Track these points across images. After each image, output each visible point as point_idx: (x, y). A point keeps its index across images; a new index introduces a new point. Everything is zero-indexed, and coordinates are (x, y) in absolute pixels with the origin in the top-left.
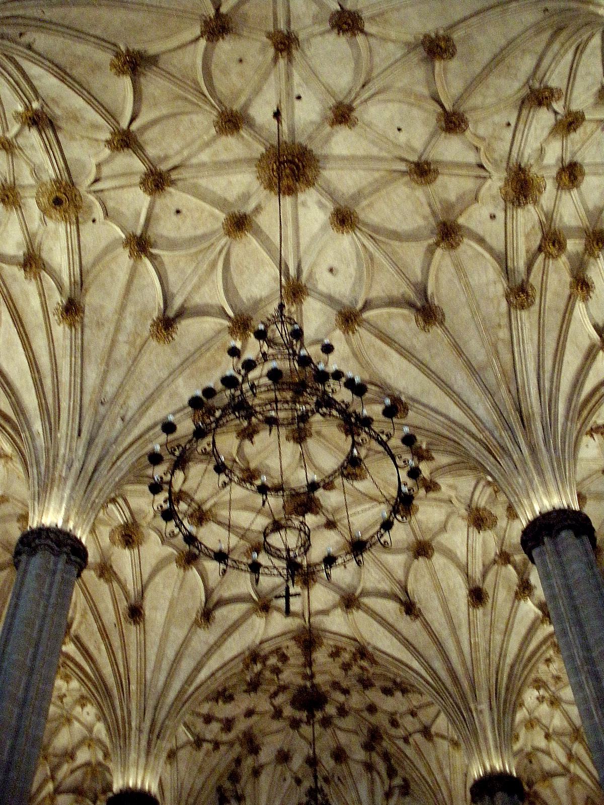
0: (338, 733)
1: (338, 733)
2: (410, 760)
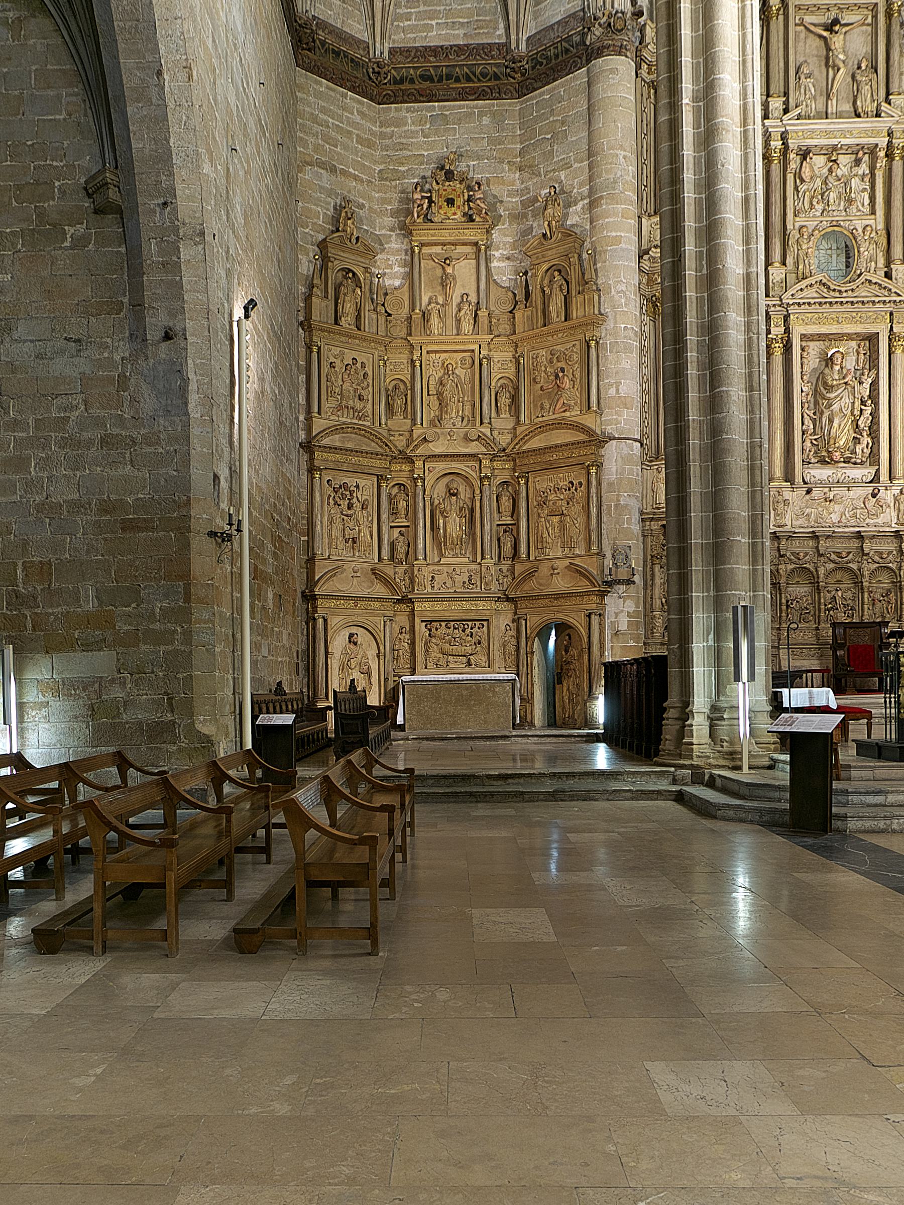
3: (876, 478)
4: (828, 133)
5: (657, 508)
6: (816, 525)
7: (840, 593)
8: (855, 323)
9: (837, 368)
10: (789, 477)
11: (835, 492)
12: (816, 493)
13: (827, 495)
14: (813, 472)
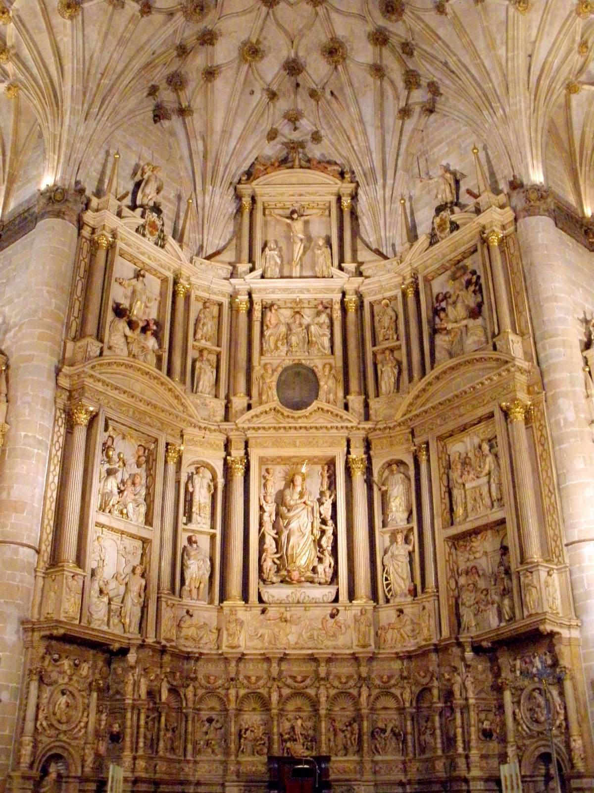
0: (334, 16)
1: (334, 16)
2: (444, 42)
3: (336, 600)
4: (285, 290)
6: (271, 646)
7: (299, 722)
8: (313, 446)
9: (298, 489)
10: (245, 597)
11: (293, 612)
12: (272, 612)
13: (284, 615)
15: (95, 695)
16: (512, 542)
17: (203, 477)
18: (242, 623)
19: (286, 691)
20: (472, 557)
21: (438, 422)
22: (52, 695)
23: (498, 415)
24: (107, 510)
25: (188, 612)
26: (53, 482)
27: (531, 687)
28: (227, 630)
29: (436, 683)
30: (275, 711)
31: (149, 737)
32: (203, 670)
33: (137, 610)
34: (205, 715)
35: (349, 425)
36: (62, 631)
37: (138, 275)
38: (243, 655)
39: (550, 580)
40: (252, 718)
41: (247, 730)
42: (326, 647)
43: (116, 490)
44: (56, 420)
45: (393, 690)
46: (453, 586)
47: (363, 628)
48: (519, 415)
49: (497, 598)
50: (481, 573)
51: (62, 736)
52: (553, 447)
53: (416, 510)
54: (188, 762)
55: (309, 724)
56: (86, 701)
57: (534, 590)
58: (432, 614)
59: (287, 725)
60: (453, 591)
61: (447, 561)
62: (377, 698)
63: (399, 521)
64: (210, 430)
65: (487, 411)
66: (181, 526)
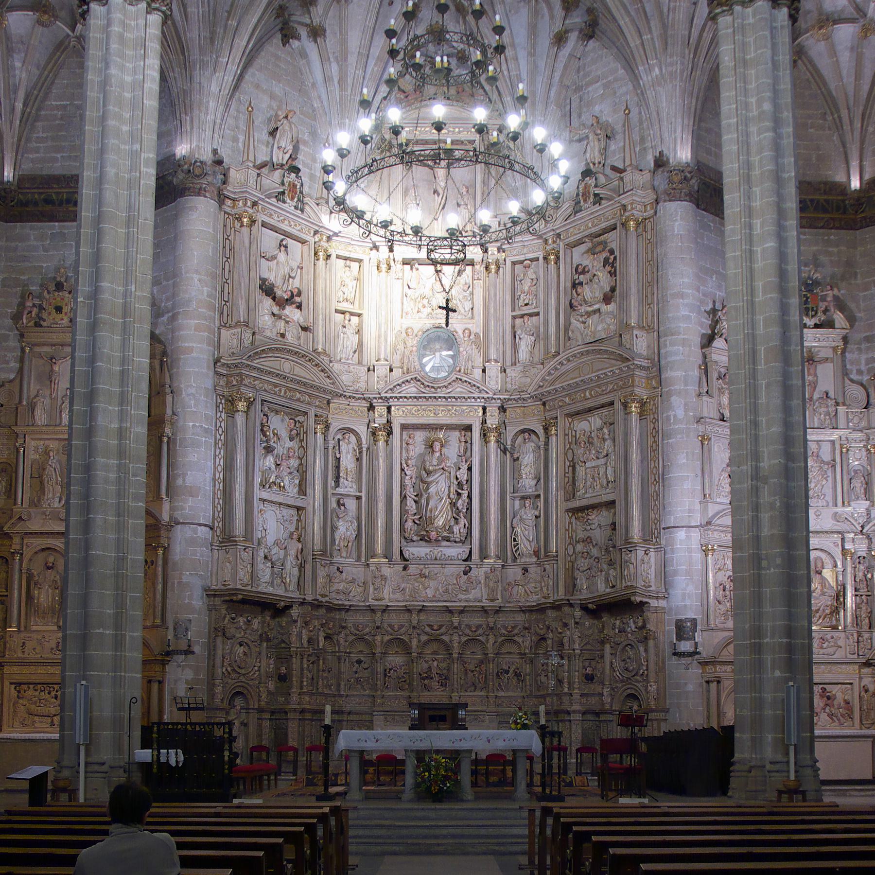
3: (469, 558)
5: (224, 585)
7: (435, 663)
12: (413, 569)
14: (411, 550)
15: (265, 644)
16: (620, 522)
17: (349, 443)
18: (384, 578)
19: (424, 638)
20: (588, 528)
21: (567, 400)
22: (232, 647)
23: (618, 405)
24: (267, 486)
25: (338, 569)
26: (219, 465)
27: (625, 643)
28: (373, 584)
29: (551, 635)
30: (414, 654)
31: (310, 676)
32: (351, 619)
33: (296, 571)
34: (355, 657)
35: (486, 396)
36: (240, 597)
37: (282, 245)
38: (388, 606)
39: (646, 558)
40: (396, 660)
41: (390, 670)
42: (461, 600)
43: (273, 467)
44: (218, 407)
45: (516, 638)
46: (571, 552)
47: (491, 584)
48: (634, 408)
49: (605, 567)
50: (594, 543)
51: (242, 678)
52: (663, 440)
53: (543, 477)
54: (342, 696)
55: (444, 665)
56: (258, 649)
57: (631, 566)
58: (551, 576)
59: (425, 665)
60: (570, 556)
61: (566, 530)
62: (502, 644)
63: (528, 487)
64: (354, 397)
65: (609, 400)
66: (330, 491)
